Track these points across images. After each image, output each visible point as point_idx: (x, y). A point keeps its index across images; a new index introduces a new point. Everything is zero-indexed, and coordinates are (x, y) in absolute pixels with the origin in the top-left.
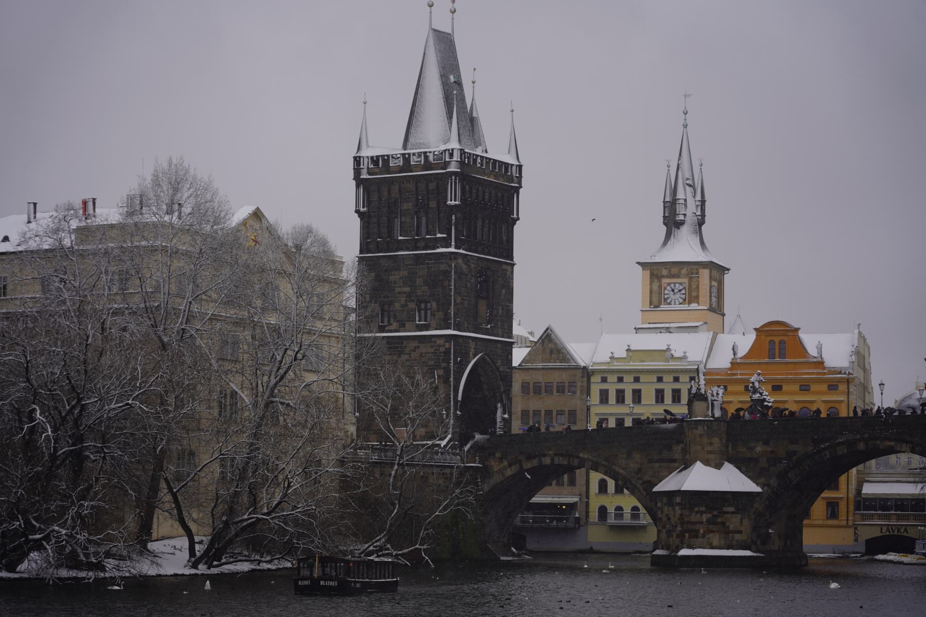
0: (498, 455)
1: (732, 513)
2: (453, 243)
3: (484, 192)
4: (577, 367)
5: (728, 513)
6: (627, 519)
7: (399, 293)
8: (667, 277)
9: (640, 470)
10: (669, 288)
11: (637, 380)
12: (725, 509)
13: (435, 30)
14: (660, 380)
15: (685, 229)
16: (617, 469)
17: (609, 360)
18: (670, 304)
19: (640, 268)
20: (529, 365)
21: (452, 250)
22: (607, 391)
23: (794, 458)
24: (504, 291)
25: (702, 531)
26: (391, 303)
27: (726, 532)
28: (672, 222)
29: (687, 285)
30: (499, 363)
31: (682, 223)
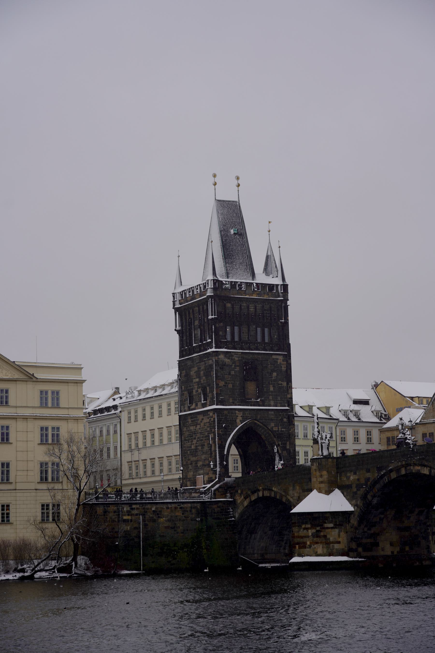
0: (239, 492)
1: (332, 528)
2: (214, 345)
3: (248, 307)
5: (328, 528)
7: (195, 383)
9: (299, 497)
12: (326, 525)
13: (219, 201)
16: (289, 498)
20: (426, 421)
21: (214, 349)
23: (369, 483)
24: (275, 374)
26: (192, 389)
27: (328, 543)
30: (273, 425)
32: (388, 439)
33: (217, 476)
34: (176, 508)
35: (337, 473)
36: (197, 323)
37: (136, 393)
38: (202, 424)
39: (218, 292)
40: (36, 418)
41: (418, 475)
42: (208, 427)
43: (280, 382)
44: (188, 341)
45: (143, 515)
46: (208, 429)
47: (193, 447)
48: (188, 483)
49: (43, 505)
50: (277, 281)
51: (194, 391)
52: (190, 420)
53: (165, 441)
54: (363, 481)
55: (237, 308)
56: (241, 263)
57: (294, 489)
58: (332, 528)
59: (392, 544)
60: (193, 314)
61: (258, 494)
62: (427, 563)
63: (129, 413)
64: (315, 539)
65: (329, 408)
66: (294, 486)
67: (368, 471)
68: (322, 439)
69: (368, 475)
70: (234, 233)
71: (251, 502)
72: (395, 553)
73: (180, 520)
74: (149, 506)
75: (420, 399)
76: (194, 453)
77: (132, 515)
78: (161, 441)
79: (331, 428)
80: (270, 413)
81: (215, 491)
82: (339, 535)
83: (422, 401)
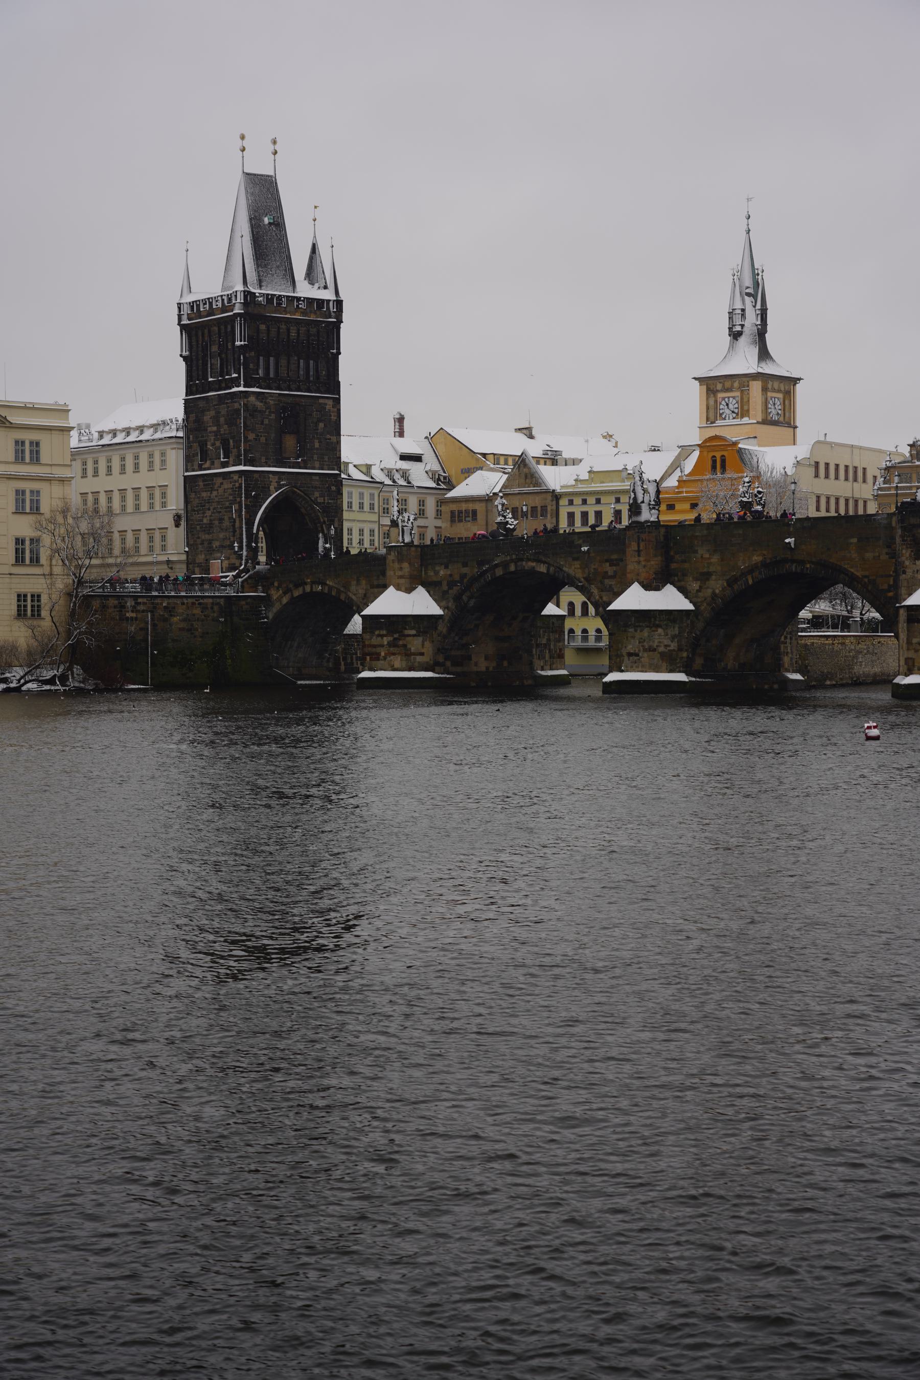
0: (276, 584)
1: (414, 636)
4: (547, 492)
6: (591, 642)
8: (722, 391)
9: (365, 595)
10: (723, 403)
11: (598, 501)
13: (247, 174)
14: (618, 500)
15: (742, 340)
16: (351, 595)
17: (574, 483)
18: (725, 419)
19: (697, 383)
20: (508, 491)
21: (241, 389)
22: (574, 513)
23: (465, 580)
24: (321, 425)
25: (383, 654)
26: (206, 441)
28: (735, 335)
29: (739, 399)
30: (317, 494)
31: (740, 334)
32: (452, 512)
33: (243, 562)
34: (193, 604)
35: (421, 565)
36: (215, 348)
37: (96, 435)
38: (221, 491)
39: (250, 310)
40: (10, 478)
41: (533, 572)
42: (230, 495)
43: (328, 436)
44: (200, 373)
45: (152, 612)
46: (231, 498)
47: (205, 521)
48: (197, 570)
49: (19, 596)
50: (328, 295)
51: (209, 443)
52: (201, 484)
53: (144, 507)
54: (457, 577)
55: (273, 331)
56: (278, 267)
57: (358, 583)
58: (414, 636)
59: (486, 658)
60: (210, 336)
61: (304, 589)
62: (530, 682)
63: (85, 463)
64: (392, 649)
65: (371, 465)
66: (358, 581)
67: (465, 565)
68: (403, 521)
69: (465, 570)
70: (270, 223)
71: (292, 598)
72: (491, 669)
73: (198, 620)
74: (159, 601)
75: (496, 457)
76: (208, 528)
77: (137, 611)
78: (137, 507)
79: (372, 495)
80: (314, 478)
81: (242, 582)
82: (423, 645)
83: (498, 459)
